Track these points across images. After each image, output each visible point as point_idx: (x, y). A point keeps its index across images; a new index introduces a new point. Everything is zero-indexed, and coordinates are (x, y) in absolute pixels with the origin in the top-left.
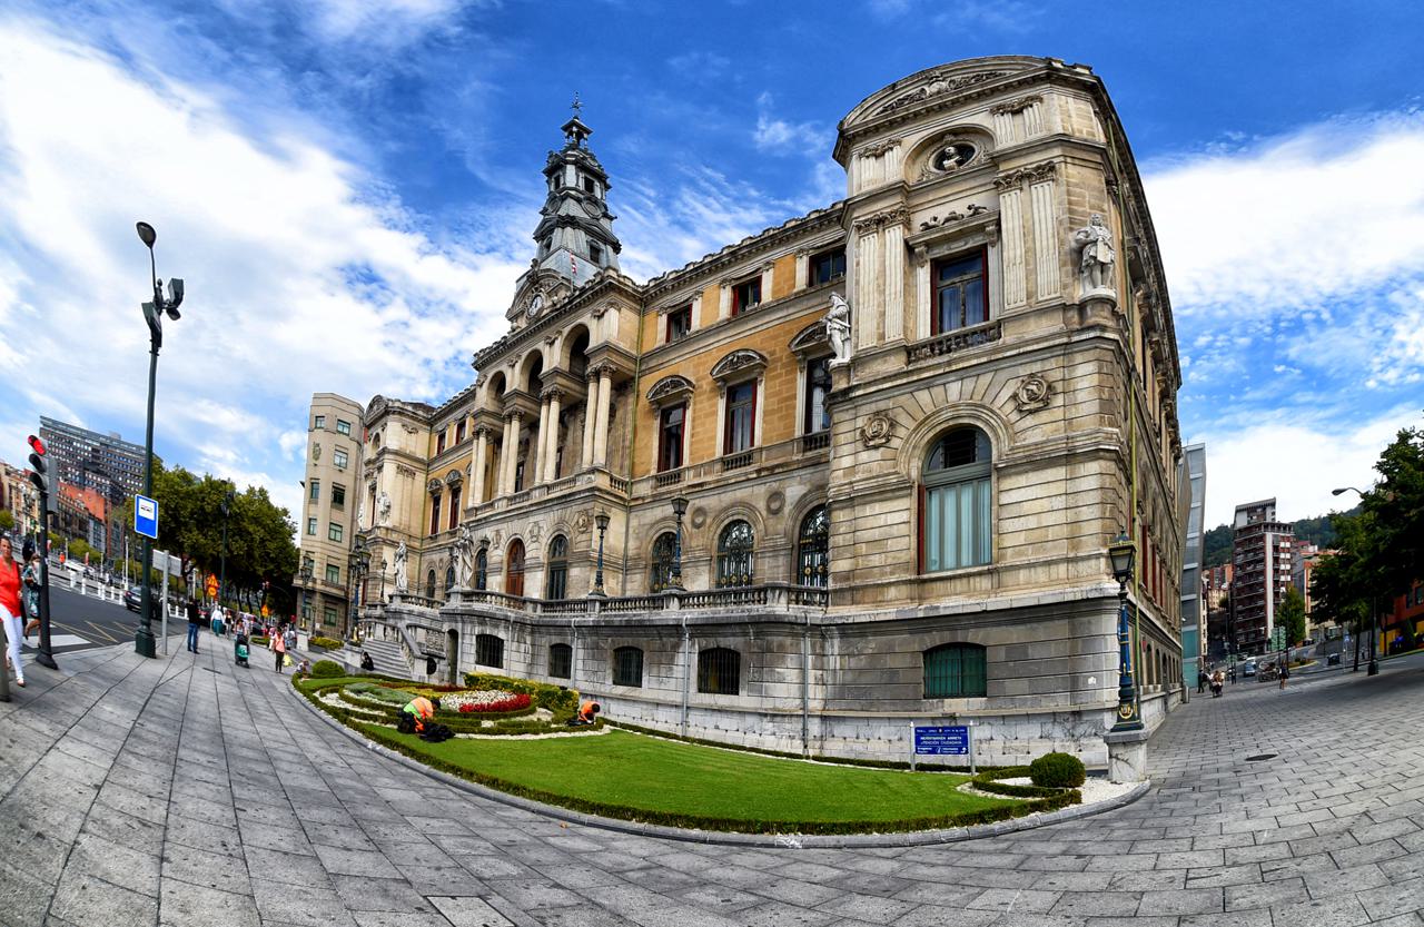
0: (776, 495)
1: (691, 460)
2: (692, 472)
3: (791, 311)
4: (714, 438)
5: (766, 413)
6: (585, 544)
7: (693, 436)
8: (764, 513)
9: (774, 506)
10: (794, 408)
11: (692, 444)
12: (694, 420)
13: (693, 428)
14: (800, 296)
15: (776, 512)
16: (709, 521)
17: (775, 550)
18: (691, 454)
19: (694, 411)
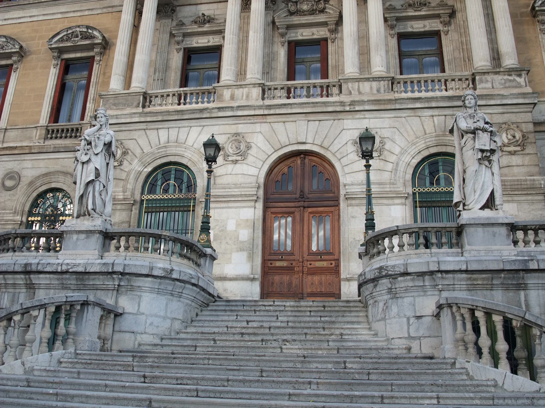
6: (523, 170)
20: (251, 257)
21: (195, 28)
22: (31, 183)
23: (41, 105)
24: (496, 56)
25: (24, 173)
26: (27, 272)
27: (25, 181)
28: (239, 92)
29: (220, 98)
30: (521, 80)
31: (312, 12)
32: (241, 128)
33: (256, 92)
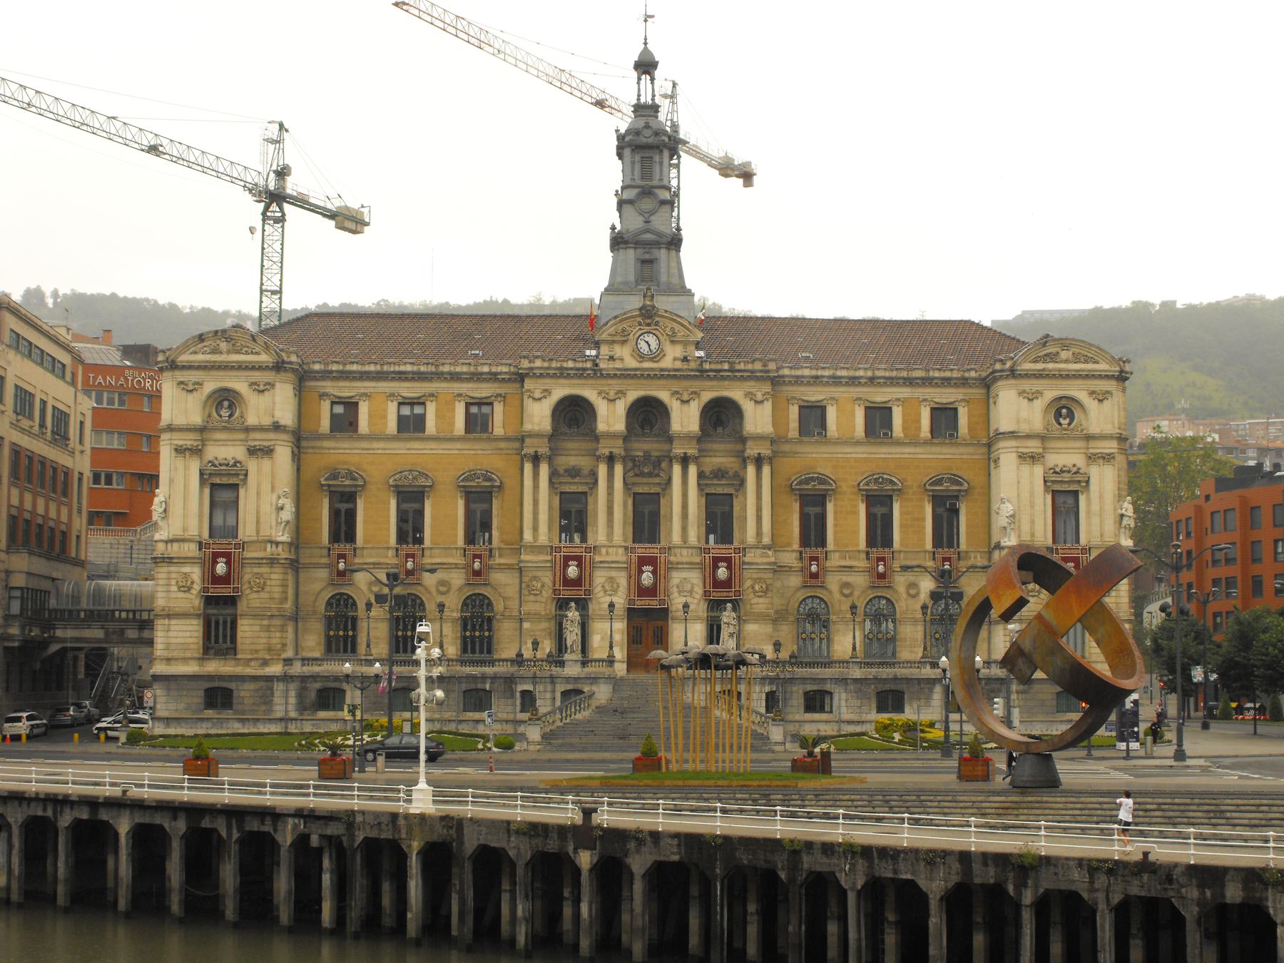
0: (913, 585)
1: (836, 544)
2: (837, 555)
3: (918, 450)
4: (856, 532)
5: (902, 526)
7: (835, 525)
8: (904, 595)
9: (912, 592)
10: (924, 527)
11: (835, 532)
12: (835, 513)
13: (835, 519)
14: (926, 443)
15: (913, 596)
16: (856, 593)
17: (915, 621)
18: (835, 539)
19: (835, 506)
20: (622, 649)
21: (569, 479)
22: (460, 589)
23: (456, 529)
24: (759, 533)
25: (453, 582)
26: (553, 679)
27: (454, 588)
28: (610, 550)
29: (600, 553)
30: (770, 553)
31: (650, 475)
32: (613, 574)
33: (621, 551)
